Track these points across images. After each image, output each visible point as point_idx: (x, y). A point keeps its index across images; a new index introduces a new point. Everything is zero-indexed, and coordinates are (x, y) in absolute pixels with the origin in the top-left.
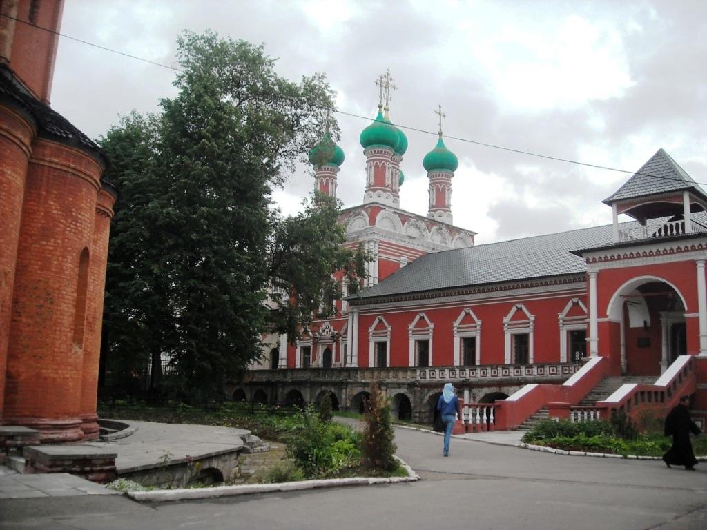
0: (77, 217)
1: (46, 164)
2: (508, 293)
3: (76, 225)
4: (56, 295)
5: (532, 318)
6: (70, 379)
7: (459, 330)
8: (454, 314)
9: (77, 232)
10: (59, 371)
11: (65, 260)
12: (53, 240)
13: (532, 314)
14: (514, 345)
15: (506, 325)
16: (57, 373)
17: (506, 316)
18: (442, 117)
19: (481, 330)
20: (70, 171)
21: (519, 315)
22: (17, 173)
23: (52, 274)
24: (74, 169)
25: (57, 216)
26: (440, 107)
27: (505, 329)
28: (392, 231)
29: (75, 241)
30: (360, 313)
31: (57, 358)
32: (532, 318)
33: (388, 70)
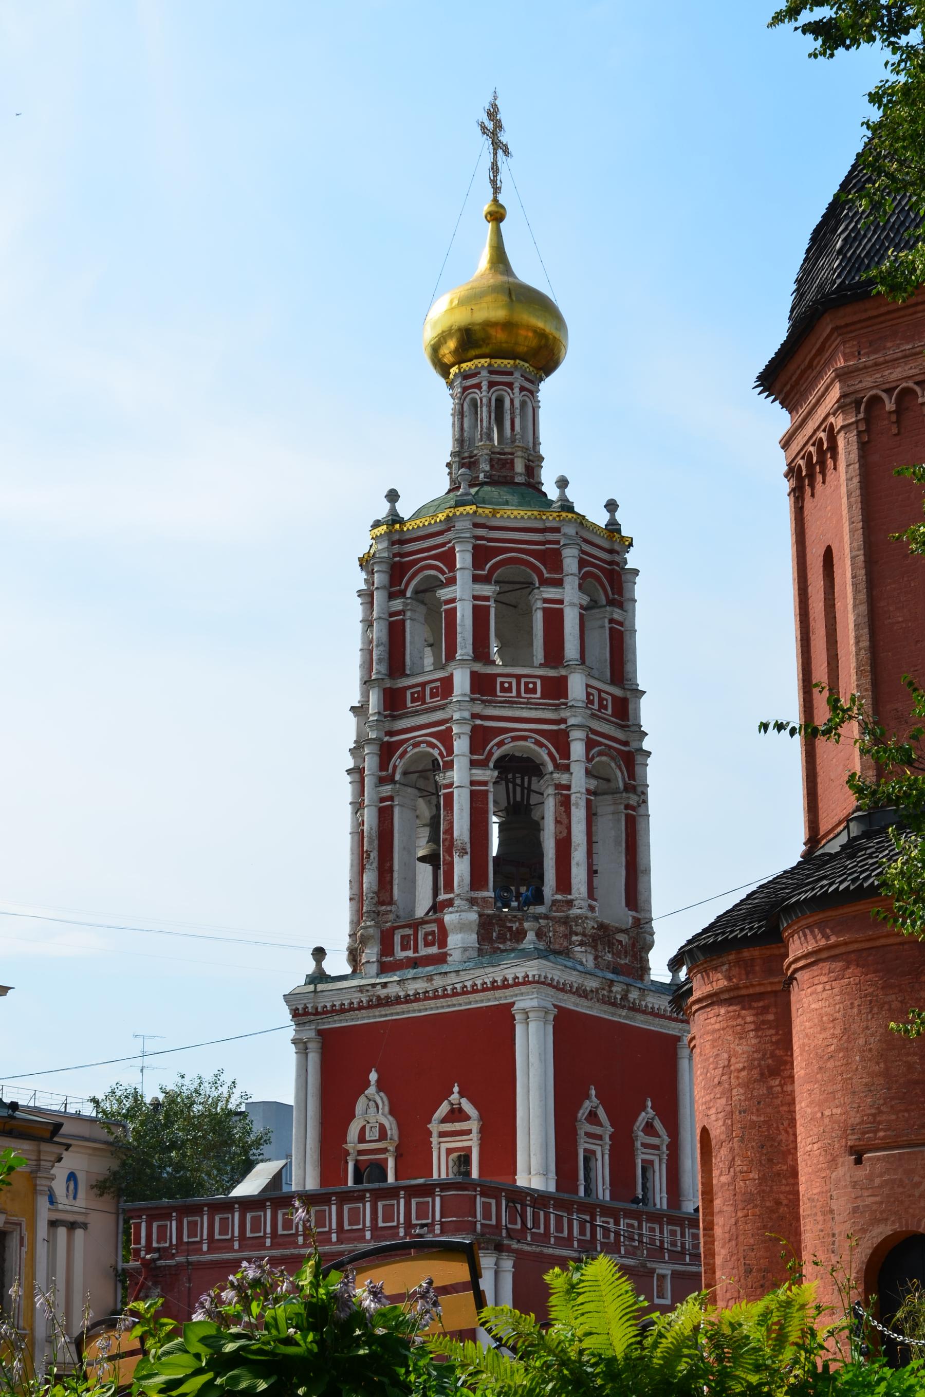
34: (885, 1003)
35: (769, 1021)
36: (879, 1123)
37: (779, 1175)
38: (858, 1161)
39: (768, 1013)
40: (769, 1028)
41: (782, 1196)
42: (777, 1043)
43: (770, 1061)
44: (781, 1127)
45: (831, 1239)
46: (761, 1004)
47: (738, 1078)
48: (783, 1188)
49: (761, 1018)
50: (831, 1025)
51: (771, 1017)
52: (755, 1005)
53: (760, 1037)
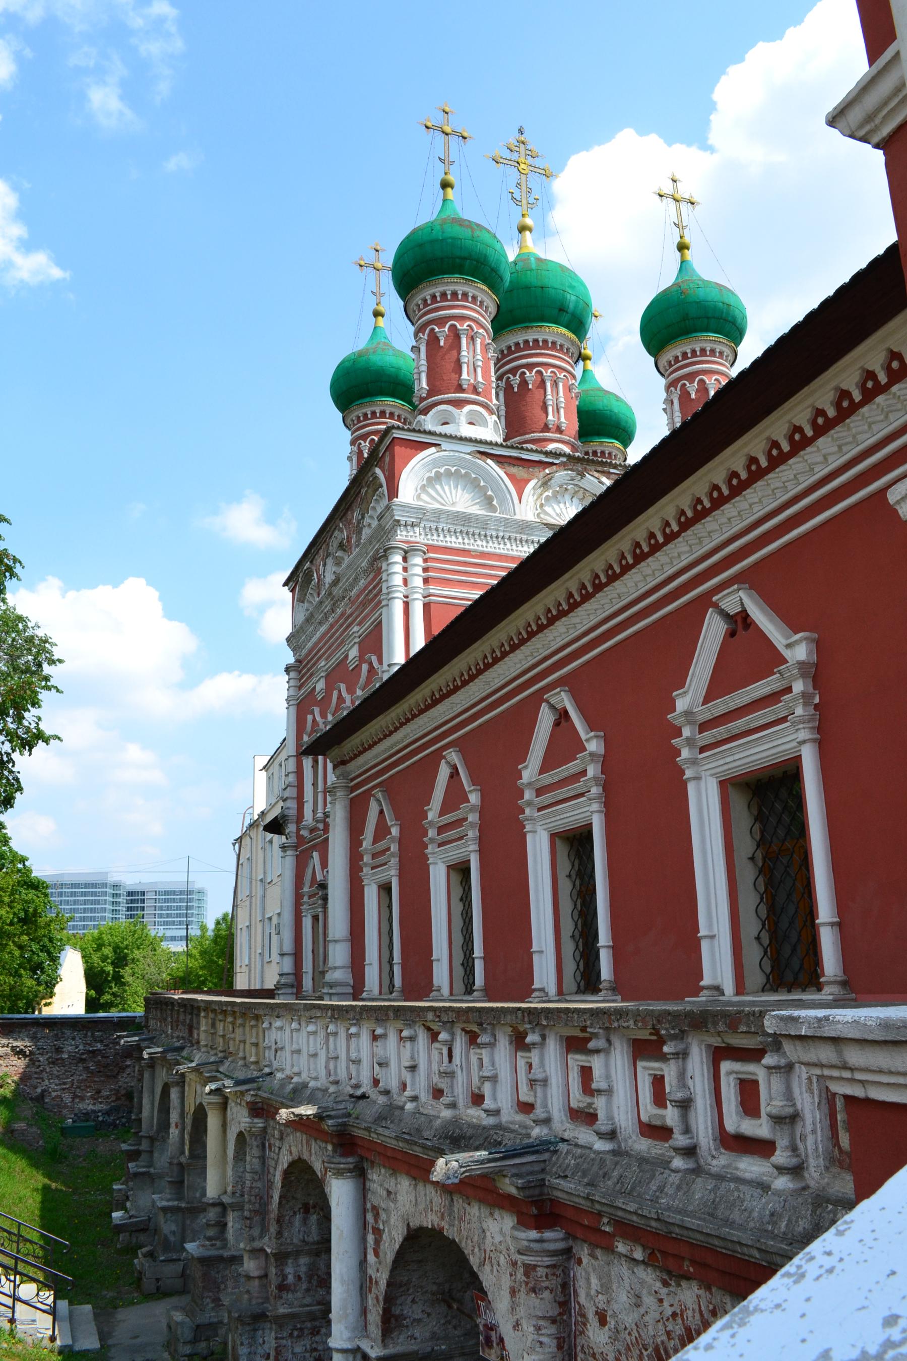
2: (681, 553)
5: (798, 651)
7: (547, 798)
8: (520, 723)
13: (794, 625)
14: (746, 846)
15: (686, 732)
17: (680, 681)
18: (684, 206)
19: (607, 787)
21: (745, 652)
26: (674, 181)
27: (685, 753)
28: (476, 510)
30: (353, 789)
32: (798, 651)
33: (521, 132)
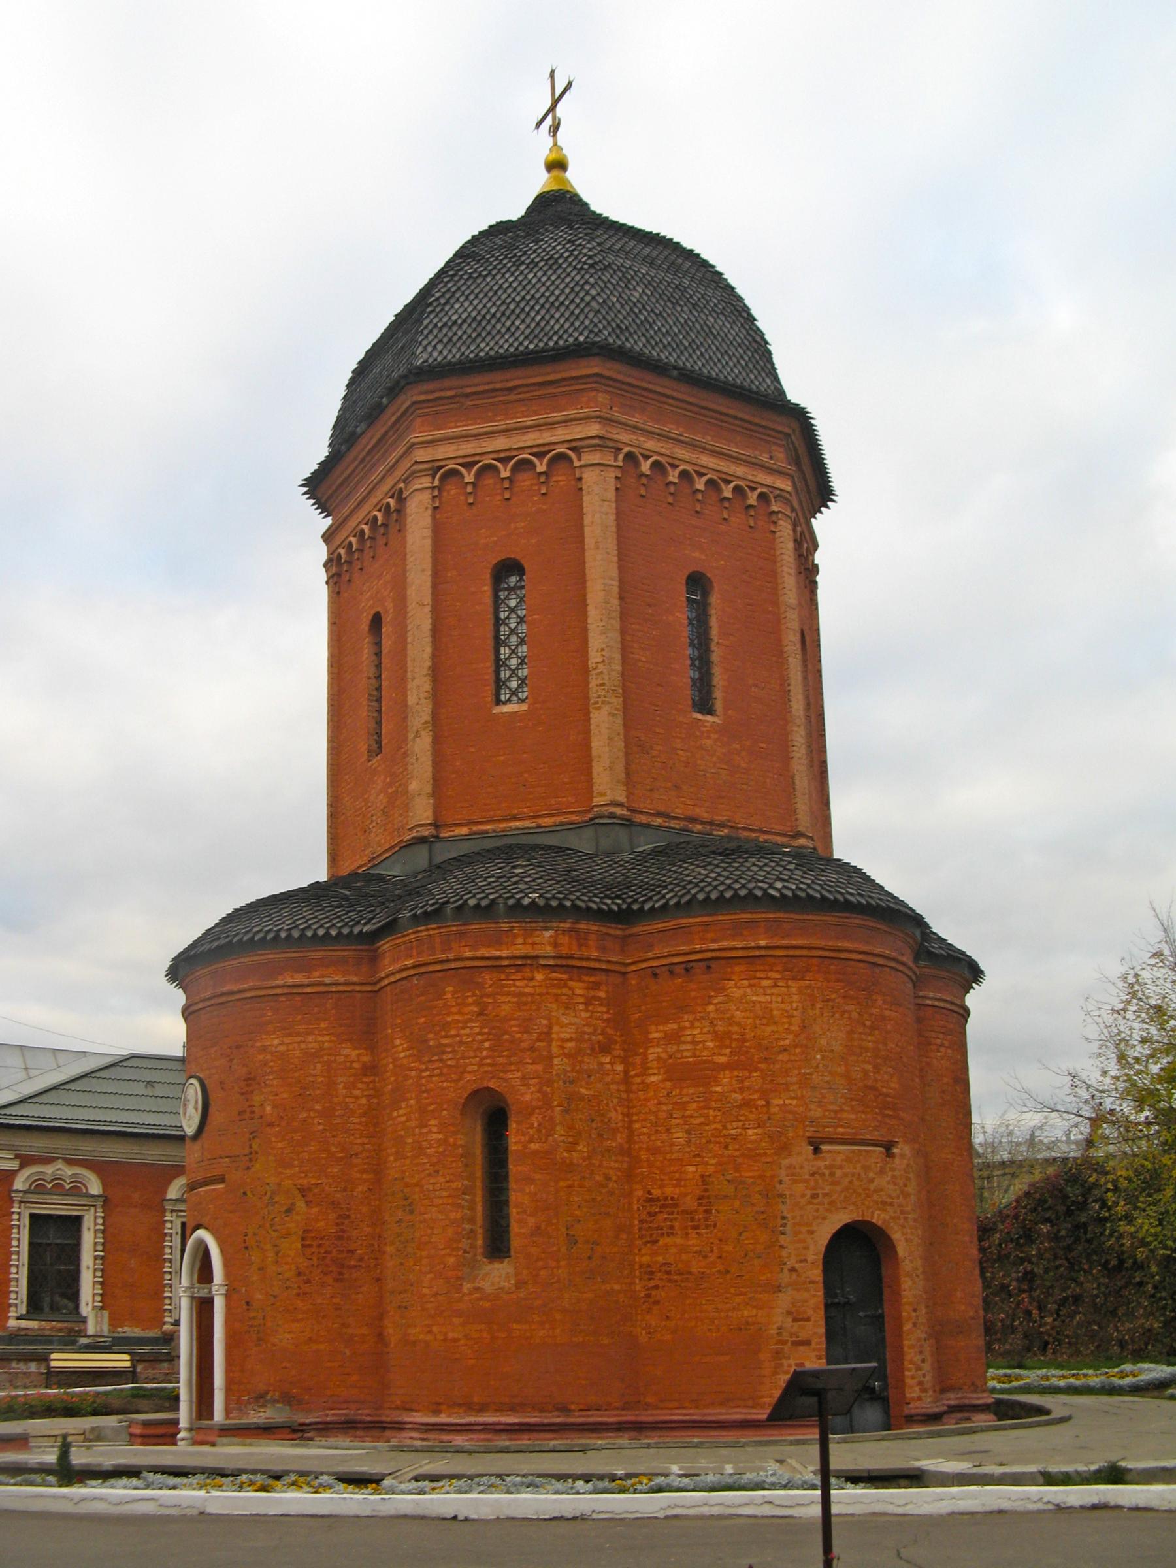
0: (440, 1045)
1: (386, 982)
3: (441, 1060)
4: (416, 1196)
6: (462, 1342)
9: (445, 1071)
10: (435, 1329)
11: (425, 1130)
12: (403, 1105)
16: (430, 1332)
20: (412, 972)
22: (298, 1034)
23: (408, 1162)
24: (414, 967)
25: (405, 1062)
29: (443, 1089)
31: (429, 1306)
34: (845, 1012)
35: (600, 999)
36: (840, 1119)
37: (609, 1151)
38: (817, 1150)
39: (599, 989)
40: (601, 1005)
41: (611, 1172)
42: (608, 1021)
43: (600, 1038)
44: (611, 1105)
45: (780, 1222)
46: (592, 979)
47: (562, 1047)
48: (613, 1164)
49: (592, 993)
50: (785, 1020)
51: (602, 994)
52: (586, 978)
53: (592, 1012)
